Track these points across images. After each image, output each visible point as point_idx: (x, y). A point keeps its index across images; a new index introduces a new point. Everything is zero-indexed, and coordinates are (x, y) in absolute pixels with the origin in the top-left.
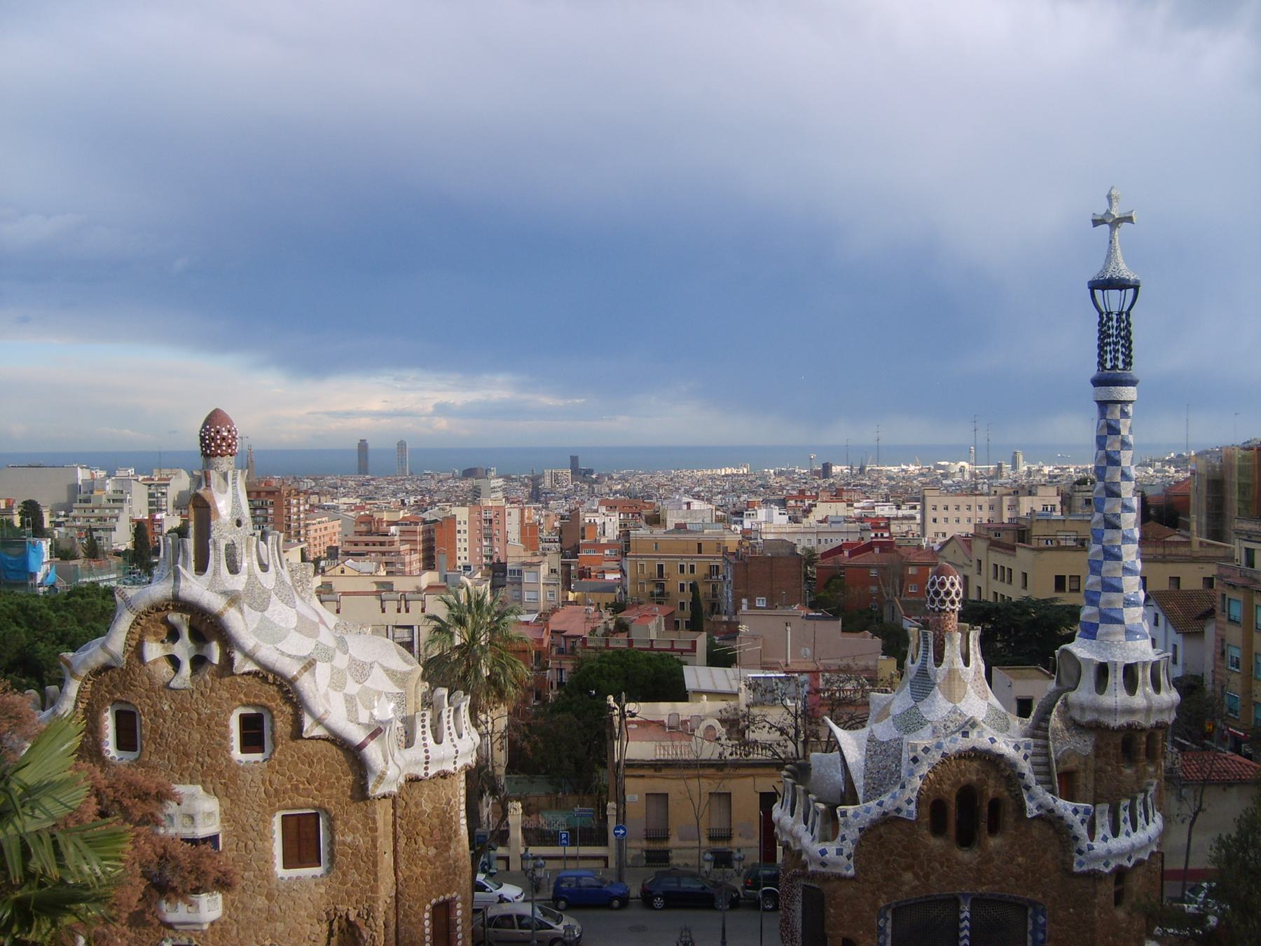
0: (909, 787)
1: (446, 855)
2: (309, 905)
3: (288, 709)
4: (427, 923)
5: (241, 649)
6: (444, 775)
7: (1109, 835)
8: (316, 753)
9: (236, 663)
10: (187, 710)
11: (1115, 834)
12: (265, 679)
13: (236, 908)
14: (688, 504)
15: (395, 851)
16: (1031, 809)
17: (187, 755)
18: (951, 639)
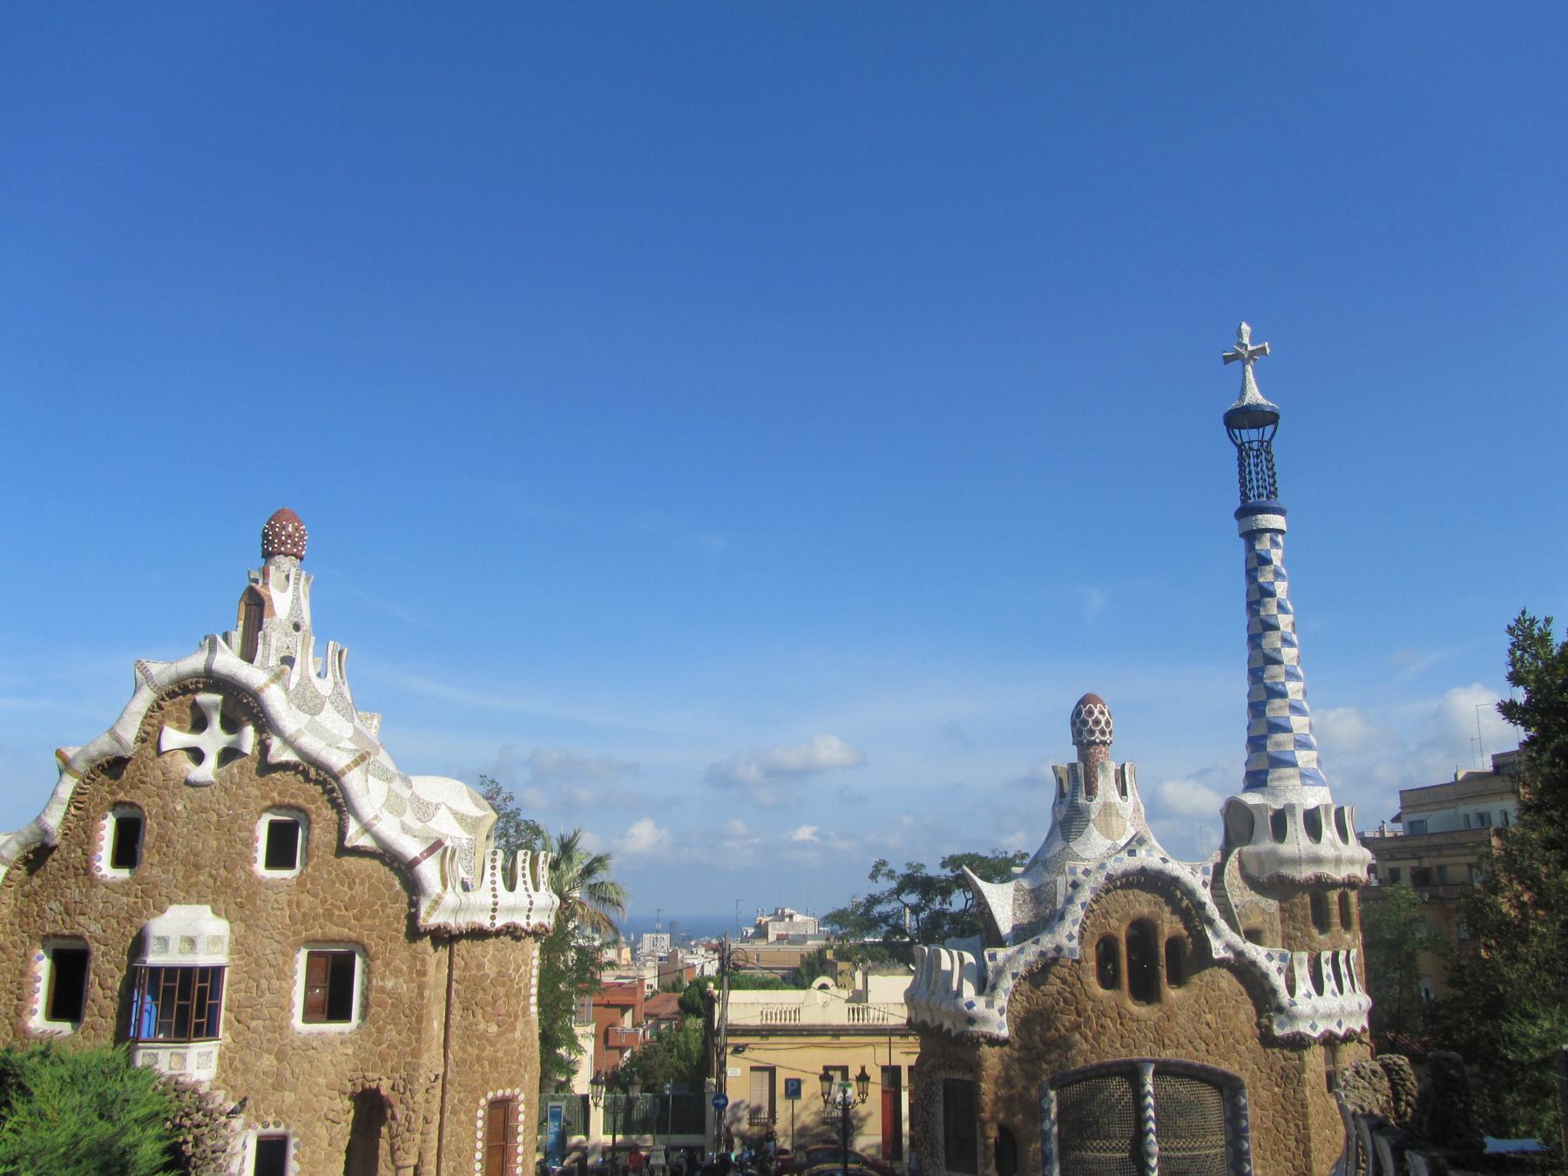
0: (1069, 918)
1: (509, 1035)
2: (331, 1069)
3: (331, 814)
4: (480, 1123)
5: (279, 733)
6: (513, 932)
7: (1313, 992)
8: (359, 871)
9: (273, 750)
10: (204, 810)
11: (1319, 989)
12: (305, 773)
13: (236, 1070)
14: (791, 916)
15: (447, 1026)
16: (1218, 950)
17: (197, 866)
18: (1104, 769)
